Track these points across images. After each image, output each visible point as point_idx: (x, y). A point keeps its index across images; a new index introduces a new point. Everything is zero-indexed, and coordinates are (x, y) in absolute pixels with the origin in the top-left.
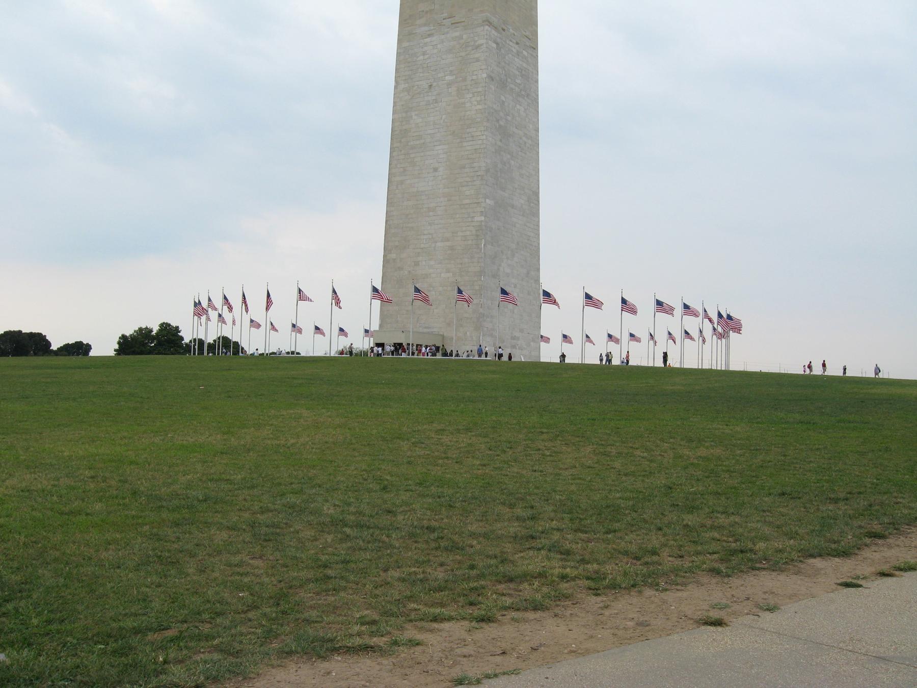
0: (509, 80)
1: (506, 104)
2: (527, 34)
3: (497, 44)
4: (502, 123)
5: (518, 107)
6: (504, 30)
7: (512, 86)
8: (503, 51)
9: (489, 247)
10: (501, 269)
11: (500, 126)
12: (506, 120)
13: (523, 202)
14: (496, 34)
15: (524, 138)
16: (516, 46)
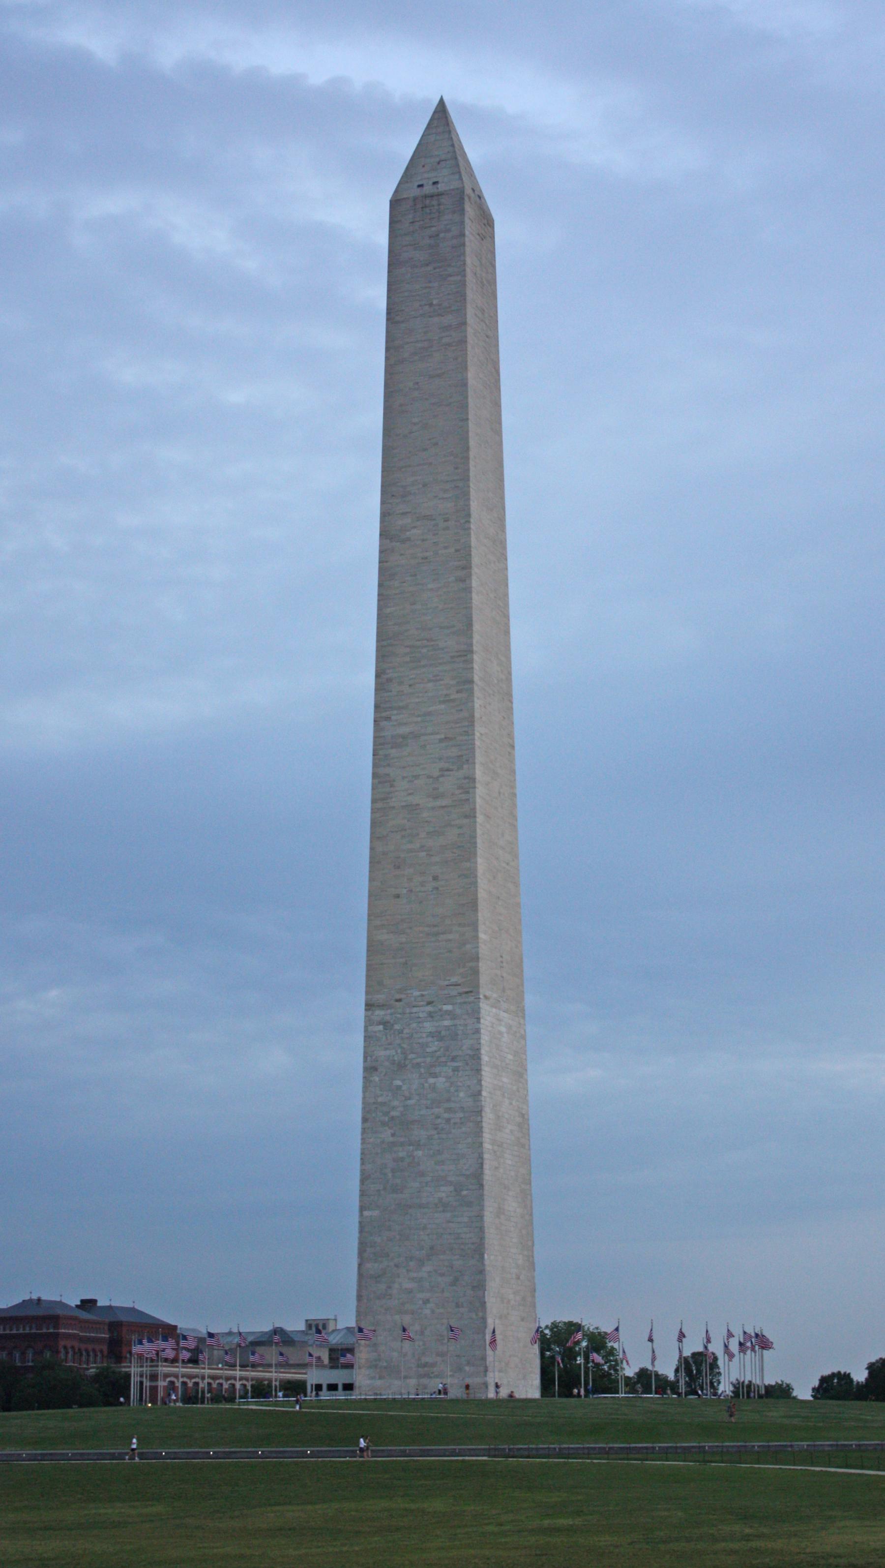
0: (411, 1056)
1: (404, 1088)
2: (454, 980)
3: (385, 1023)
4: (393, 1113)
5: (432, 1080)
6: (399, 1000)
7: (419, 1060)
8: (397, 1027)
9: (369, 1265)
10: (396, 1286)
11: (393, 1118)
12: (405, 1106)
13: (443, 1195)
14: (382, 1013)
15: (446, 1115)
16: (430, 1008)
